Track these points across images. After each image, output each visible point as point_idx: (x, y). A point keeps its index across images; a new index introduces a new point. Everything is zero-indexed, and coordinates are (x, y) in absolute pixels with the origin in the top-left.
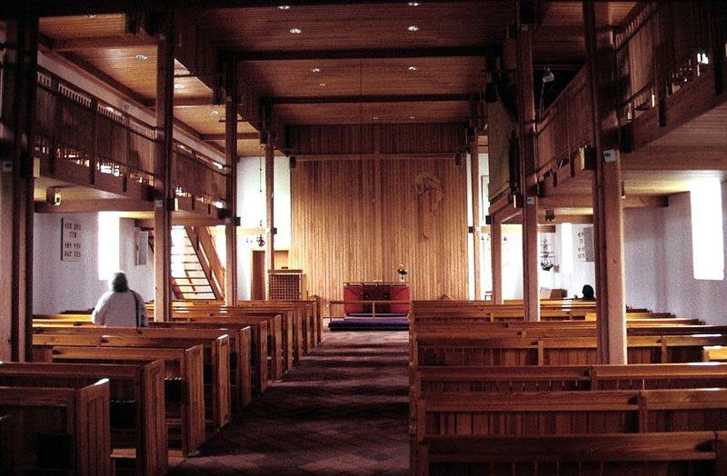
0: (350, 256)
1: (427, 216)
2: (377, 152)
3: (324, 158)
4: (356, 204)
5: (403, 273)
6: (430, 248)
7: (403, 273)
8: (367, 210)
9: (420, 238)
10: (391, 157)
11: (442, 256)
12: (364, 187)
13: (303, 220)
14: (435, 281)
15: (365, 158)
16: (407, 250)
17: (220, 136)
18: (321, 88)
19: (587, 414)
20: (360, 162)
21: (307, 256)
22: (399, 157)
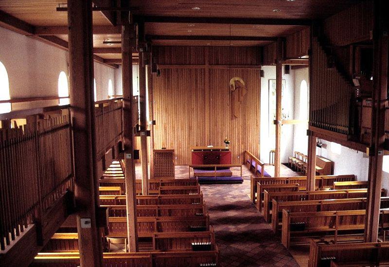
0: (190, 128)
1: (237, 104)
2: (207, 63)
3: (174, 67)
4: (194, 98)
5: (228, 143)
6: (238, 123)
7: (228, 143)
8: (200, 100)
9: (232, 116)
10: (216, 67)
11: (245, 129)
12: (198, 85)
13: (161, 106)
14: (241, 143)
15: (199, 67)
16: (223, 125)
17: (60, 28)
18: (188, 33)
19: (292, 199)
20: (196, 70)
21: (163, 130)
22: (221, 67)
